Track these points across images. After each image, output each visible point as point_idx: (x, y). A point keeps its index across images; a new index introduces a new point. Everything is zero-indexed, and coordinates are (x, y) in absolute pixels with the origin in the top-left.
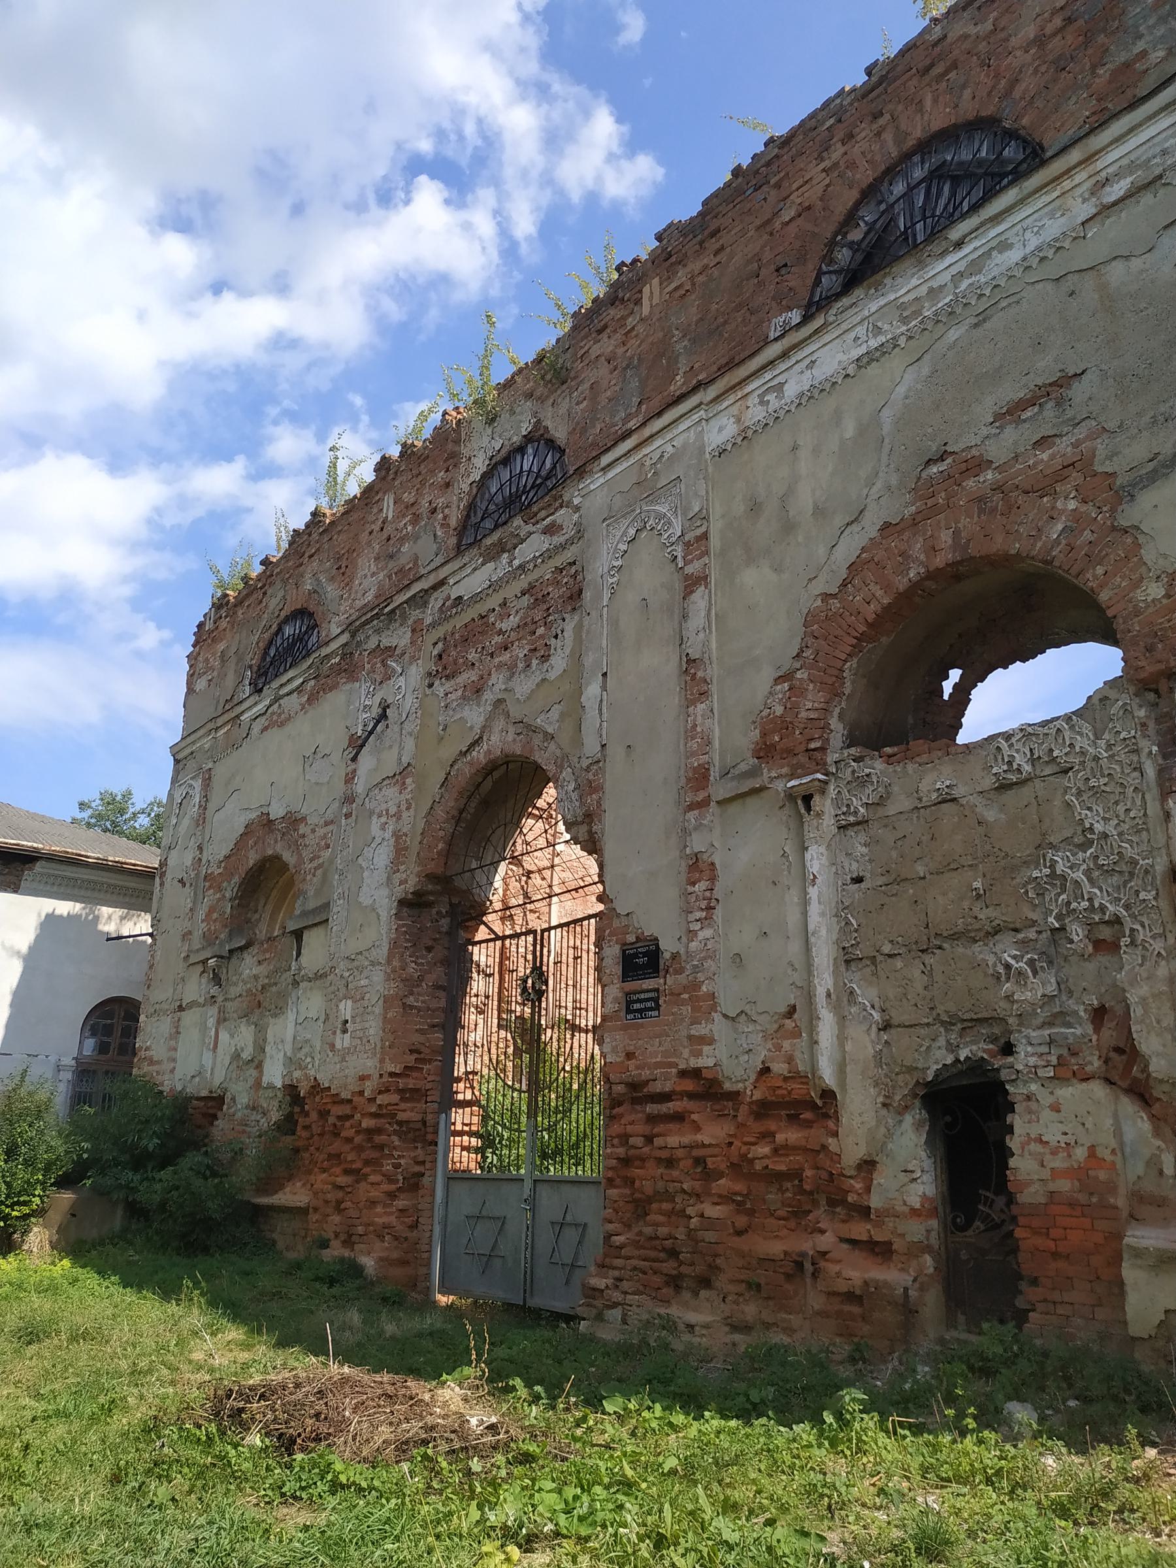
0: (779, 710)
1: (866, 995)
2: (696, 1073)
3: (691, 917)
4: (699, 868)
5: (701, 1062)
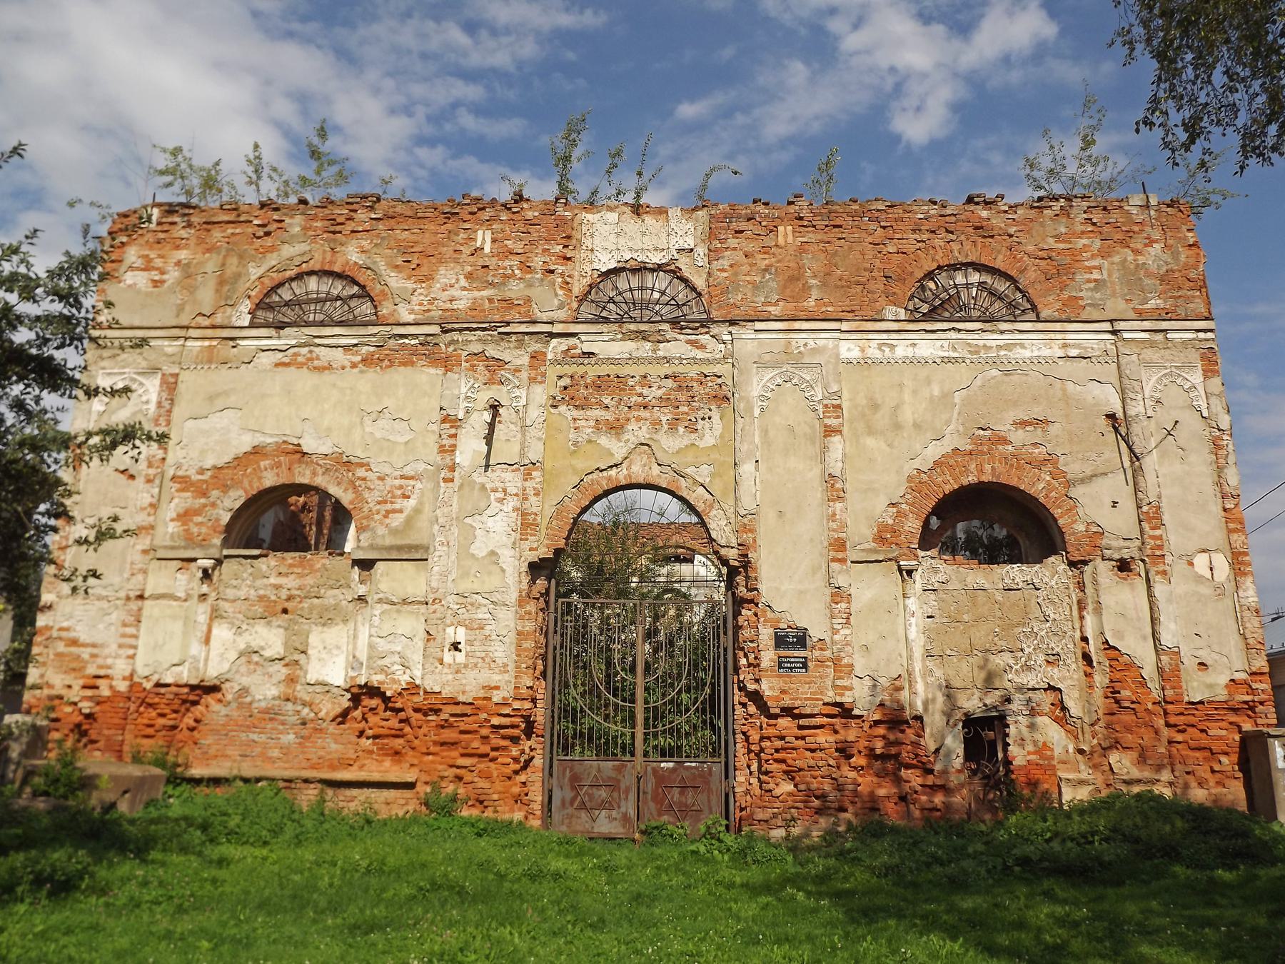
0: (890, 522)
1: (939, 673)
4: (838, 595)
5: (843, 700)
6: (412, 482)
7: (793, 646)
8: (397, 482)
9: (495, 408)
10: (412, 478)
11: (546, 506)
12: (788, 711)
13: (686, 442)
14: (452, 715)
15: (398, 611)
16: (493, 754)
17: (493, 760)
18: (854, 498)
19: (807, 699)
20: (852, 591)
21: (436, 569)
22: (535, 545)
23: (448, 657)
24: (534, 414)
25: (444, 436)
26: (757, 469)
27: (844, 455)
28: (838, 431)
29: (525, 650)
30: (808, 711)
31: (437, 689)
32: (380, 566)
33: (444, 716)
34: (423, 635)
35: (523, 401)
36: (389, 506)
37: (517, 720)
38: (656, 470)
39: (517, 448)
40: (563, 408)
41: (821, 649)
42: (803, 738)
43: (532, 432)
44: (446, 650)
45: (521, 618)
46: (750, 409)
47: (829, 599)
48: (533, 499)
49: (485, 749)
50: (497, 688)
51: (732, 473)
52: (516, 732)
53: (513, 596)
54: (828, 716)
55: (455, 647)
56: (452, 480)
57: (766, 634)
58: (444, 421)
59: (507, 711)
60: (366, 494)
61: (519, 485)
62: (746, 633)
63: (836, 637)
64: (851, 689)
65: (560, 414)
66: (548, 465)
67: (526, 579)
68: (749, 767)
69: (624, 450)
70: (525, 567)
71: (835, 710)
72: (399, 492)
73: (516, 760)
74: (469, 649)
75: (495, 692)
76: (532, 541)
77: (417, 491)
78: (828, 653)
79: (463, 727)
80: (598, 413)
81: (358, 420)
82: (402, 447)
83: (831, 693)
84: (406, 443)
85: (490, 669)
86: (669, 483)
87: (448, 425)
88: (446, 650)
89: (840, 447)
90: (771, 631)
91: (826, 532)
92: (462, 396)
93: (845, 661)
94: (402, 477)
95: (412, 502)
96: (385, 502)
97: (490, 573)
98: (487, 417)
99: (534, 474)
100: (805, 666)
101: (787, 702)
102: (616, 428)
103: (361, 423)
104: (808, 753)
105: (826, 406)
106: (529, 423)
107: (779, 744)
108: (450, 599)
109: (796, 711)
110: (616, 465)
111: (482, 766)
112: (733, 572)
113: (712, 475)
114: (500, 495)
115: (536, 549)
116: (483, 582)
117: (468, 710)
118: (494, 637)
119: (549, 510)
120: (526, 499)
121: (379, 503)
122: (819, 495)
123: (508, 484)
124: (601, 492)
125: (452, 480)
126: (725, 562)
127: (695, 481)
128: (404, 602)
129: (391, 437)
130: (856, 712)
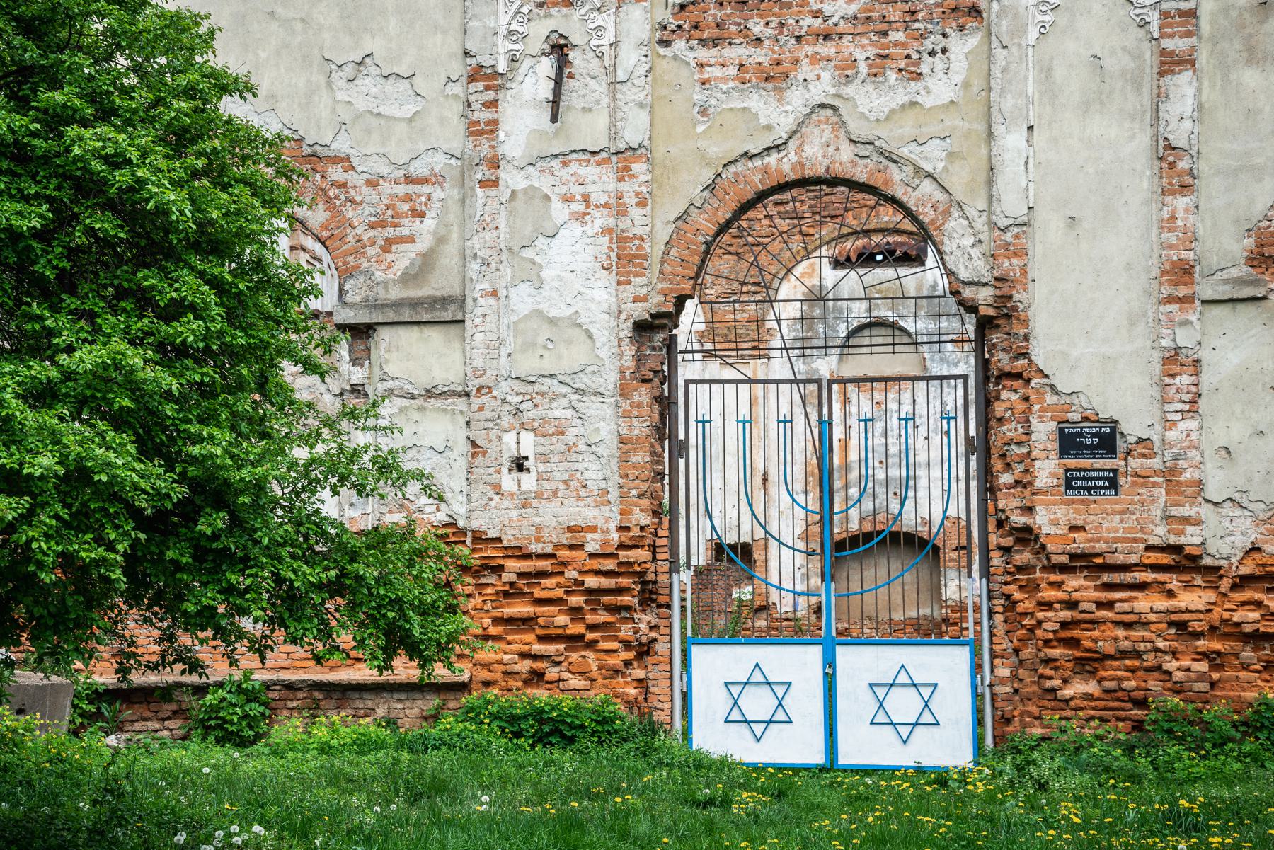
2: (1177, 549)
3: (1167, 407)
5: (1183, 540)
6: (426, 189)
7: (1093, 451)
8: (401, 189)
9: (560, 49)
10: (425, 181)
11: (659, 225)
12: (1083, 562)
13: (901, 97)
14: (521, 575)
15: (421, 409)
16: (590, 636)
17: (592, 645)
18: (1212, 188)
19: (1117, 540)
20: (1205, 354)
21: (479, 337)
22: (643, 291)
23: (508, 482)
24: (631, 59)
25: (475, 106)
26: (1030, 143)
27: (1200, 107)
28: (1185, 61)
29: (634, 467)
30: (1119, 559)
31: (492, 534)
32: (384, 334)
33: (506, 577)
34: (462, 447)
35: (609, 37)
36: (389, 232)
37: (625, 581)
38: (847, 153)
39: (602, 121)
40: (679, 45)
41: (1144, 456)
42: (1110, 605)
43: (630, 94)
44: (505, 470)
45: (626, 415)
46: (1022, 30)
47: (1157, 368)
48: (635, 212)
49: (578, 629)
50: (593, 529)
51: (984, 152)
52: (626, 599)
53: (609, 380)
54: (1156, 568)
55: (519, 465)
56: (495, 183)
57: (1044, 432)
58: (472, 78)
59: (610, 565)
60: (350, 213)
61: (611, 188)
62: (1009, 430)
63: (1172, 435)
64: (1198, 522)
65: (675, 58)
66: (659, 153)
67: (629, 351)
68: (1016, 651)
69: (791, 119)
70: (627, 330)
71: (1164, 559)
72: (405, 207)
73: (627, 645)
74: (541, 467)
75: (589, 536)
76: (638, 286)
77: (436, 204)
78: (1155, 463)
79: (538, 593)
80: (739, 52)
81: (322, 80)
82: (403, 127)
83: (1160, 530)
84: (410, 120)
85: (579, 498)
86: (871, 174)
87: (480, 85)
88: (505, 470)
89: (1190, 91)
90: (1053, 425)
91: (1157, 251)
92: (503, 31)
93: (1187, 475)
94: (409, 180)
95: (429, 223)
96: (382, 224)
97: (569, 342)
98: (547, 66)
99: (636, 167)
100: (1113, 484)
101: (1081, 542)
102: (774, 77)
103: (329, 84)
104: (1121, 633)
105: (1166, 14)
106: (621, 76)
107: (1065, 615)
108: (505, 386)
109: (1099, 560)
110: (777, 147)
111: (574, 656)
112: (985, 325)
113: (951, 156)
114: (579, 207)
115: (644, 299)
116: (560, 357)
117: (545, 565)
118: (582, 447)
119: (664, 232)
120: (625, 213)
121: (372, 226)
122: (1145, 184)
123: (591, 188)
124: (751, 195)
125: (495, 183)
126: (972, 309)
127: (918, 170)
128: (429, 393)
129: (382, 110)
130: (1207, 561)
